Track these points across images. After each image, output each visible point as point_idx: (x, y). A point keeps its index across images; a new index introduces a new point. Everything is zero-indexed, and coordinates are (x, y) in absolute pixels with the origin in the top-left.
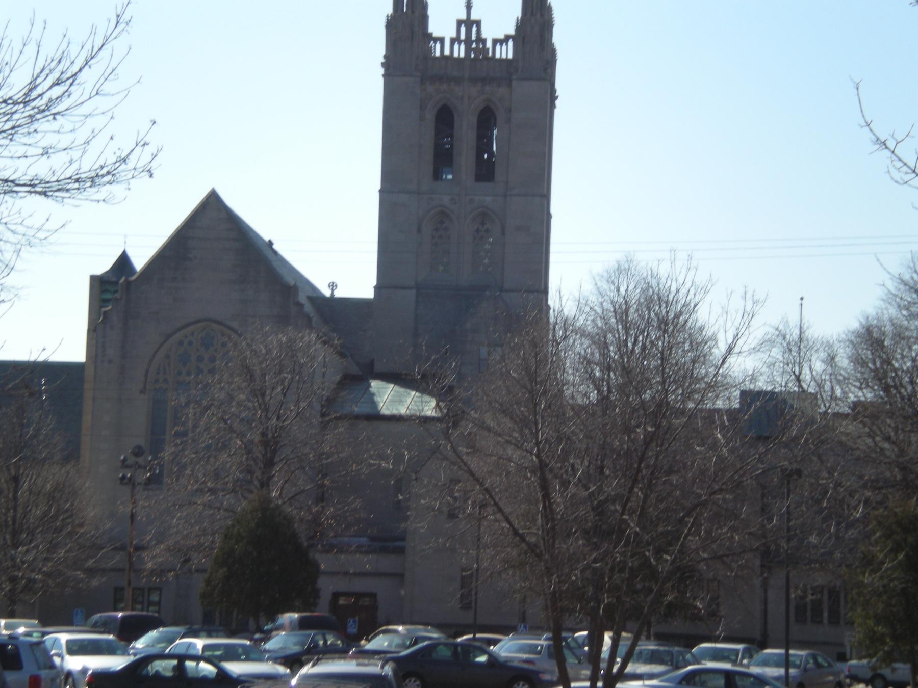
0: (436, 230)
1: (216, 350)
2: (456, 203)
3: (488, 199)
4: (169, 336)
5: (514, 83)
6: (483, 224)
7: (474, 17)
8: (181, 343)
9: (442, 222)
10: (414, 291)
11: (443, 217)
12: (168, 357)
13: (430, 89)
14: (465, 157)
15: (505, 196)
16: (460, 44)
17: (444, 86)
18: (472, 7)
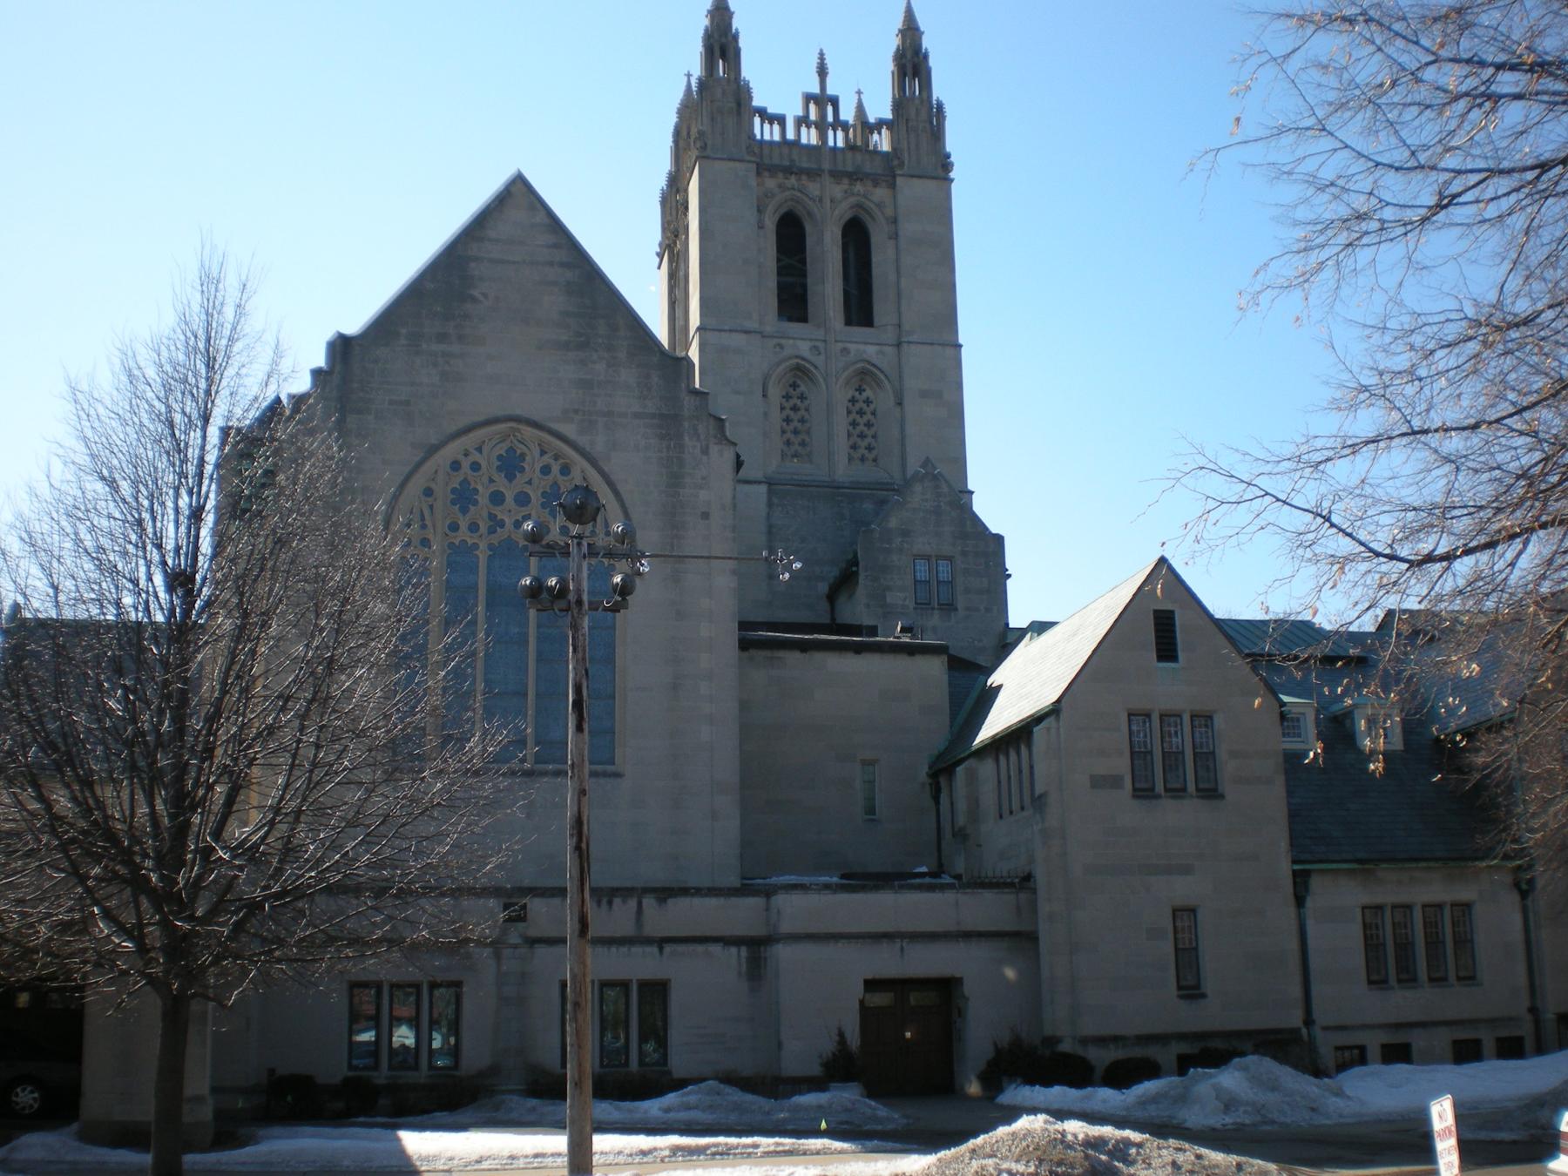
0: (787, 397)
1: (530, 482)
2: (820, 354)
3: (871, 351)
4: (433, 450)
5: (899, 181)
6: (860, 390)
7: (830, 91)
8: (456, 466)
9: (794, 386)
10: (763, 489)
11: (800, 372)
12: (428, 492)
13: (771, 183)
14: (828, 288)
15: (899, 345)
16: (808, 127)
17: (793, 180)
18: (827, 73)
